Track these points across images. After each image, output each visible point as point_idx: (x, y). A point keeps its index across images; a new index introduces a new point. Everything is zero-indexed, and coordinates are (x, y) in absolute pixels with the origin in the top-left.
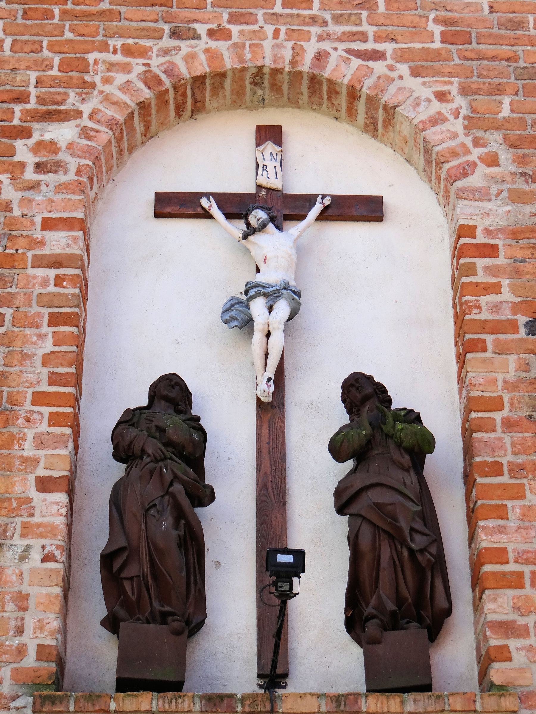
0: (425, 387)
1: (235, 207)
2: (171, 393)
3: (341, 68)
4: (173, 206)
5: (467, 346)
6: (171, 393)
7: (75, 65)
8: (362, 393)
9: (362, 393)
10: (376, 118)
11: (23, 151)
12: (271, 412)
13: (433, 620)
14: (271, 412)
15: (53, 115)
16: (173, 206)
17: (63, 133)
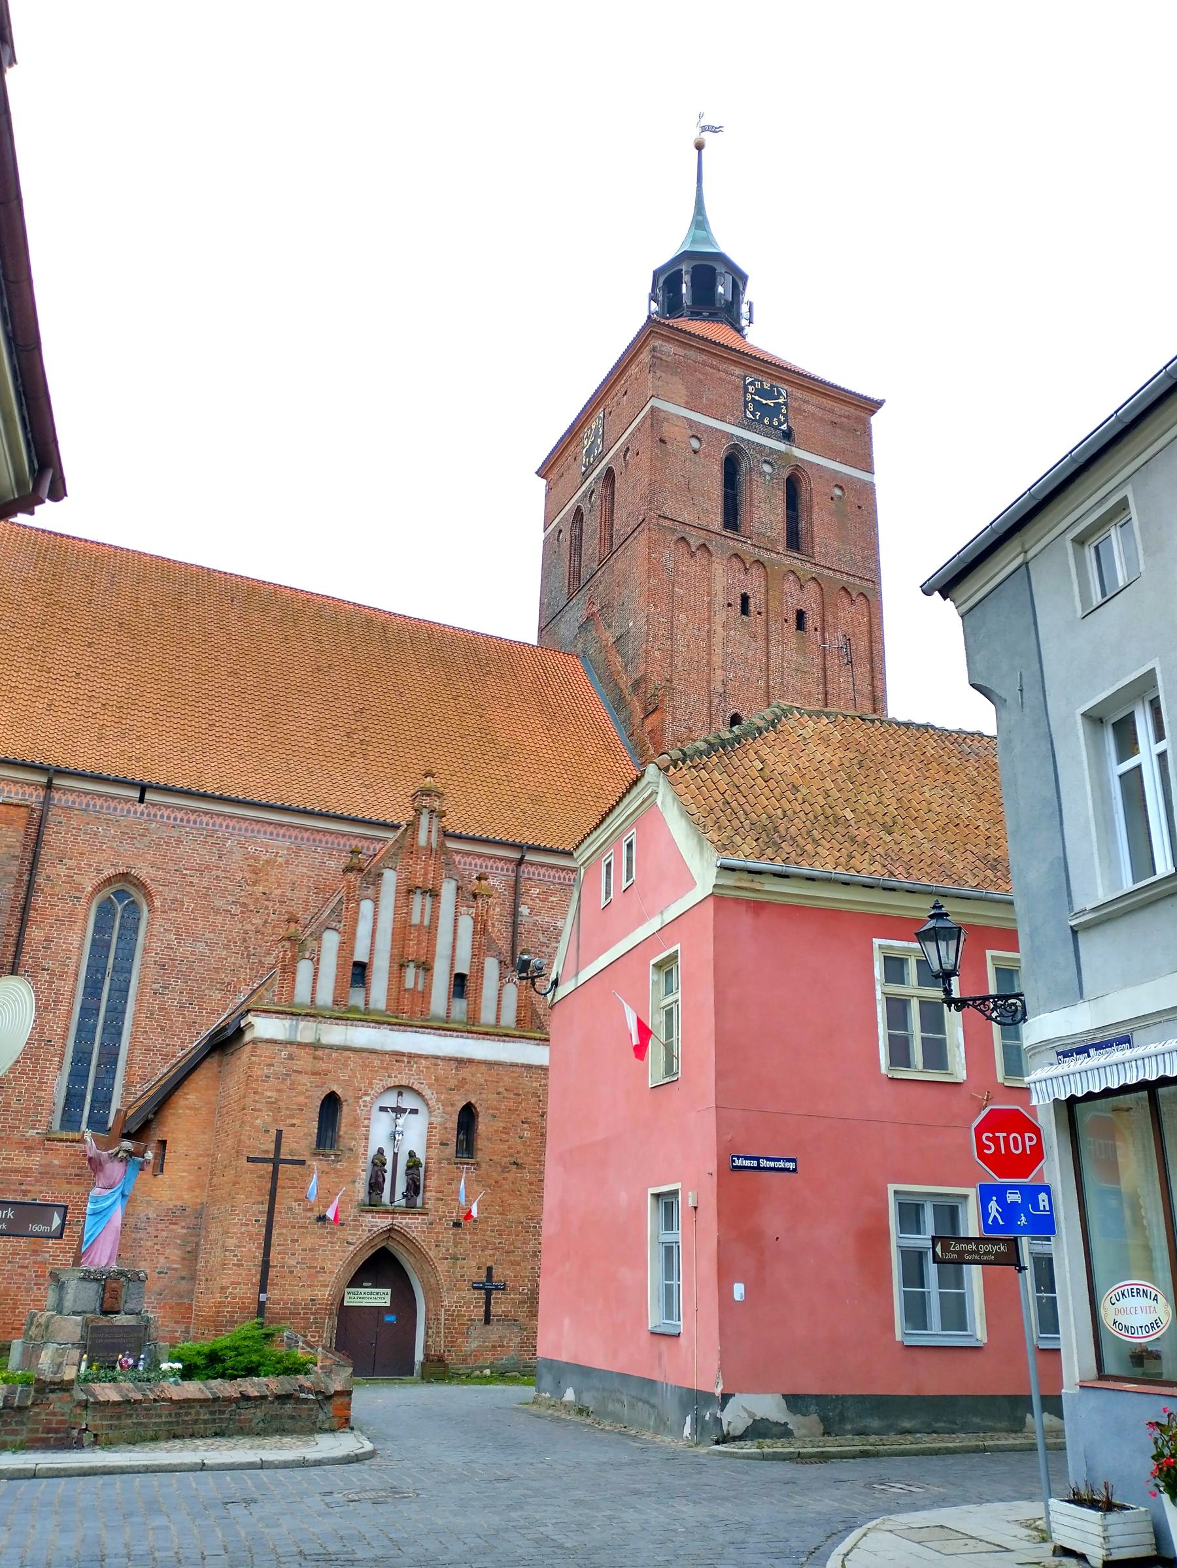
0: (421, 1156)
1: (393, 1110)
2: (381, 1151)
3: (416, 1087)
4: (383, 1109)
5: (429, 1147)
6: (381, 1151)
7: (371, 1083)
8: (412, 1154)
9: (412, 1154)
10: (419, 1094)
11: (361, 1103)
12: (396, 1155)
13: (417, 1192)
14: (396, 1155)
15: (366, 1094)
16: (383, 1109)
17: (367, 1098)
